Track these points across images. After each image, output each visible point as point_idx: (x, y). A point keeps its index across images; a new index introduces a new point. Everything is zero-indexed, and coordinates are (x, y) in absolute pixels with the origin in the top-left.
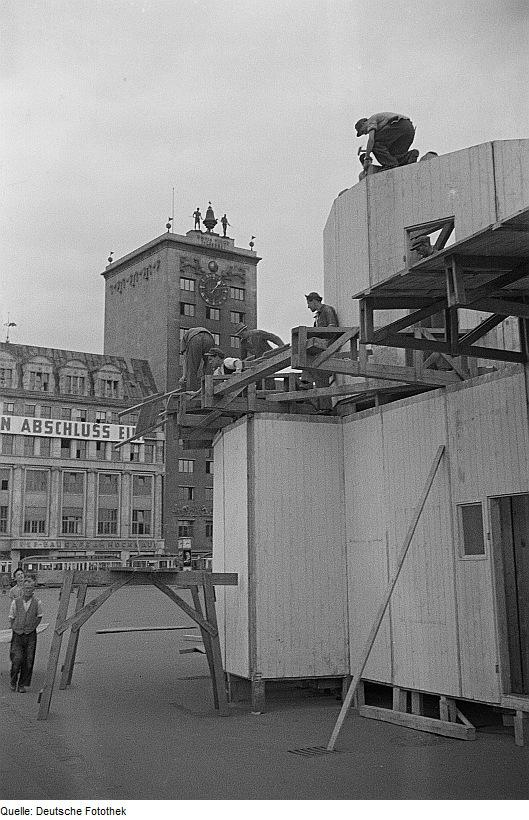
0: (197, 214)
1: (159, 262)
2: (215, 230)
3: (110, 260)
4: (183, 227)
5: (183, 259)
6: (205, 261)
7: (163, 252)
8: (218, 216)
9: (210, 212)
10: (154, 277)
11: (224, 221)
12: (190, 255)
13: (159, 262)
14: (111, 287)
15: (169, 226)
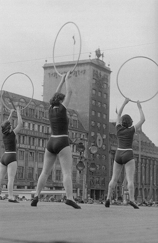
0: (96, 51)
1: (85, 71)
2: (101, 58)
3: (46, 61)
4: (94, 57)
5: (94, 71)
6: (99, 71)
7: (87, 68)
8: (101, 54)
9: (99, 51)
10: (81, 76)
11: (103, 54)
12: (95, 69)
13: (85, 71)
14: (49, 74)
15: (90, 56)
